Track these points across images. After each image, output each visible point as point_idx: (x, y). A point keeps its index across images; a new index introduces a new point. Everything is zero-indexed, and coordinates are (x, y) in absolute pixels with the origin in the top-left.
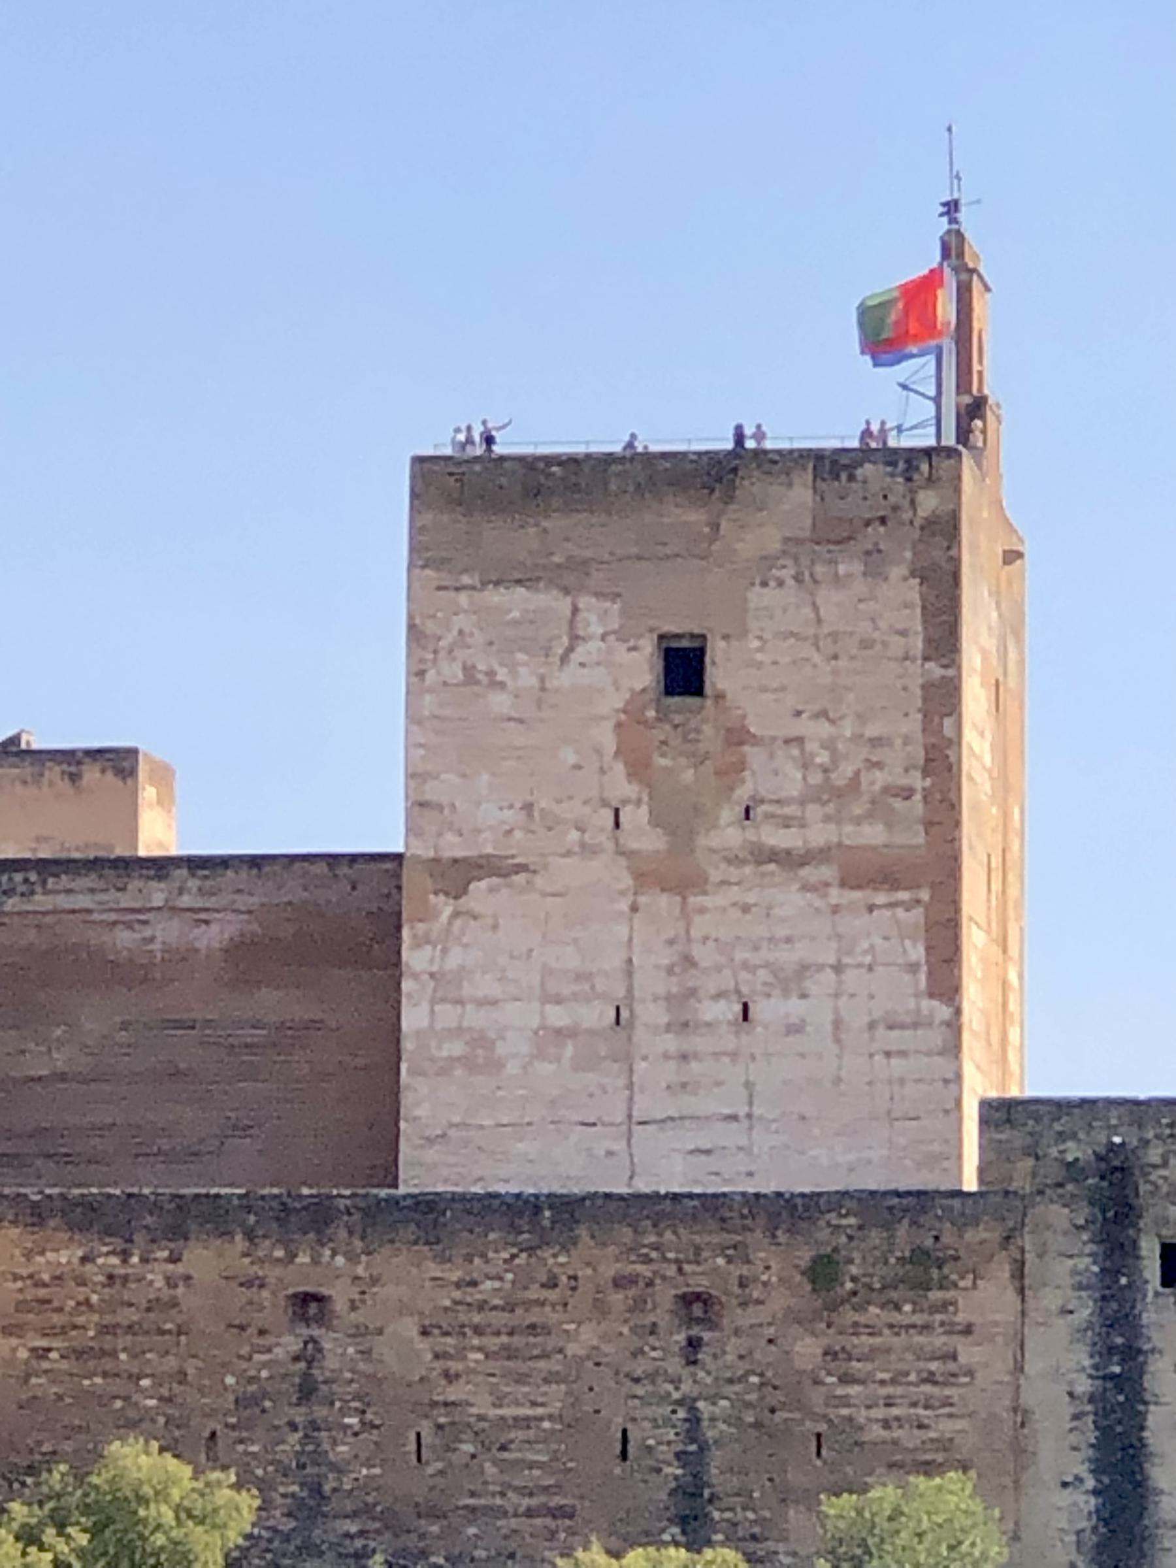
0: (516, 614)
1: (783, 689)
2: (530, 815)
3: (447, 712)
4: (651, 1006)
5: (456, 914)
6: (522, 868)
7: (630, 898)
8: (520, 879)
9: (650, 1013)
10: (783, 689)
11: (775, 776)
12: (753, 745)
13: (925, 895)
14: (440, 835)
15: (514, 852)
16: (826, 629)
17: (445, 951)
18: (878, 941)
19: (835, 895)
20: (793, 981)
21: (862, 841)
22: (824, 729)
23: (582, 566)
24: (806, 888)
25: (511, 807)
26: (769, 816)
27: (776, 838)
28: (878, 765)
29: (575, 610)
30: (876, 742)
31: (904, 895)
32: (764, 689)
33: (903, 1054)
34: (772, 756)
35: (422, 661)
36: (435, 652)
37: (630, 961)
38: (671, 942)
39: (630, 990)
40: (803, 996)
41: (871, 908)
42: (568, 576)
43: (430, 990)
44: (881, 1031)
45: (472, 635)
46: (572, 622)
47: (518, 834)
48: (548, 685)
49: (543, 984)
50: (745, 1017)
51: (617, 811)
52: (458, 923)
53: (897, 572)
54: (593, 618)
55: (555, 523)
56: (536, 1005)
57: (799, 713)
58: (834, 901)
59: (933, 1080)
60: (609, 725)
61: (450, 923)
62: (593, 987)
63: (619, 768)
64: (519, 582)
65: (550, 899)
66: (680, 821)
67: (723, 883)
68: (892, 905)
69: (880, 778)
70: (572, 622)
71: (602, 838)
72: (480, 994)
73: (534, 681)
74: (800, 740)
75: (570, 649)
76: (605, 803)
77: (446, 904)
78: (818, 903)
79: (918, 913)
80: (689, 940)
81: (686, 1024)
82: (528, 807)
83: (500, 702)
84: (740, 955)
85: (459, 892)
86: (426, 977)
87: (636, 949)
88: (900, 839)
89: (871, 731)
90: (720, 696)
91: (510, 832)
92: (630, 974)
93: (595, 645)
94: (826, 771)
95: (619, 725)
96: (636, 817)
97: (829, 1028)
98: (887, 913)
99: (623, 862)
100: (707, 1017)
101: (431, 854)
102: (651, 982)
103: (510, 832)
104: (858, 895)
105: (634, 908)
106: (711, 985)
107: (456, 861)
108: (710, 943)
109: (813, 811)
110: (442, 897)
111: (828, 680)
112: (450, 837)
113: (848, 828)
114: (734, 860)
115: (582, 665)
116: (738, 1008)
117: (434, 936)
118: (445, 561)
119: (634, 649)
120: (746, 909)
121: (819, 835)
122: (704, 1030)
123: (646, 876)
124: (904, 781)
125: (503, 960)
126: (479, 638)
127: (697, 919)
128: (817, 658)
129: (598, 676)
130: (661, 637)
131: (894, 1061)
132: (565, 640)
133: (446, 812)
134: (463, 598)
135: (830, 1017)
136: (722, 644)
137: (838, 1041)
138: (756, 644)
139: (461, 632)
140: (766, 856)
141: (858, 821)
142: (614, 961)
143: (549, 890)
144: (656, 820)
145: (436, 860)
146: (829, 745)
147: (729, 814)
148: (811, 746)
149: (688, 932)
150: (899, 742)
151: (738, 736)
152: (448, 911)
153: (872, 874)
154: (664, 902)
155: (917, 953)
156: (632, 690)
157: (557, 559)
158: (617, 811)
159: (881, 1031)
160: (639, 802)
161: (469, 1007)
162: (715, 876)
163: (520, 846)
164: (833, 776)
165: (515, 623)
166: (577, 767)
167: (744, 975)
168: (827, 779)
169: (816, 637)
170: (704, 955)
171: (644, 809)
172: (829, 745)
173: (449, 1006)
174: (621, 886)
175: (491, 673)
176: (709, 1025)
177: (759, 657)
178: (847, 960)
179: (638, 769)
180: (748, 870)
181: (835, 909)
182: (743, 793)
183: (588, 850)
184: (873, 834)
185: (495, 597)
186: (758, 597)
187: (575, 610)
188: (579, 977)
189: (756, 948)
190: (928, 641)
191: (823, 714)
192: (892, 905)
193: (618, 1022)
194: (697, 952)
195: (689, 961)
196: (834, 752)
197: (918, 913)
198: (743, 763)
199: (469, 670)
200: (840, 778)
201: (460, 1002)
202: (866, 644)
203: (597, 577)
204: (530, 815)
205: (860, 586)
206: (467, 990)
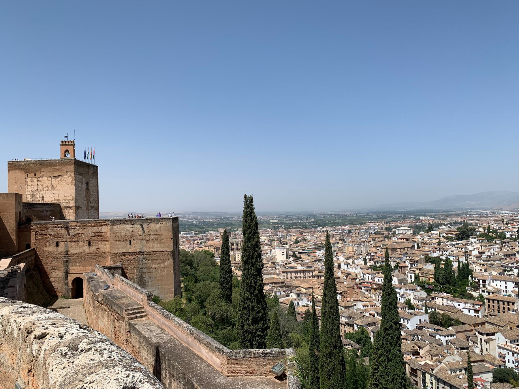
23: (82, 174)
140: (92, 207)
151: (90, 194)
186: (91, 179)
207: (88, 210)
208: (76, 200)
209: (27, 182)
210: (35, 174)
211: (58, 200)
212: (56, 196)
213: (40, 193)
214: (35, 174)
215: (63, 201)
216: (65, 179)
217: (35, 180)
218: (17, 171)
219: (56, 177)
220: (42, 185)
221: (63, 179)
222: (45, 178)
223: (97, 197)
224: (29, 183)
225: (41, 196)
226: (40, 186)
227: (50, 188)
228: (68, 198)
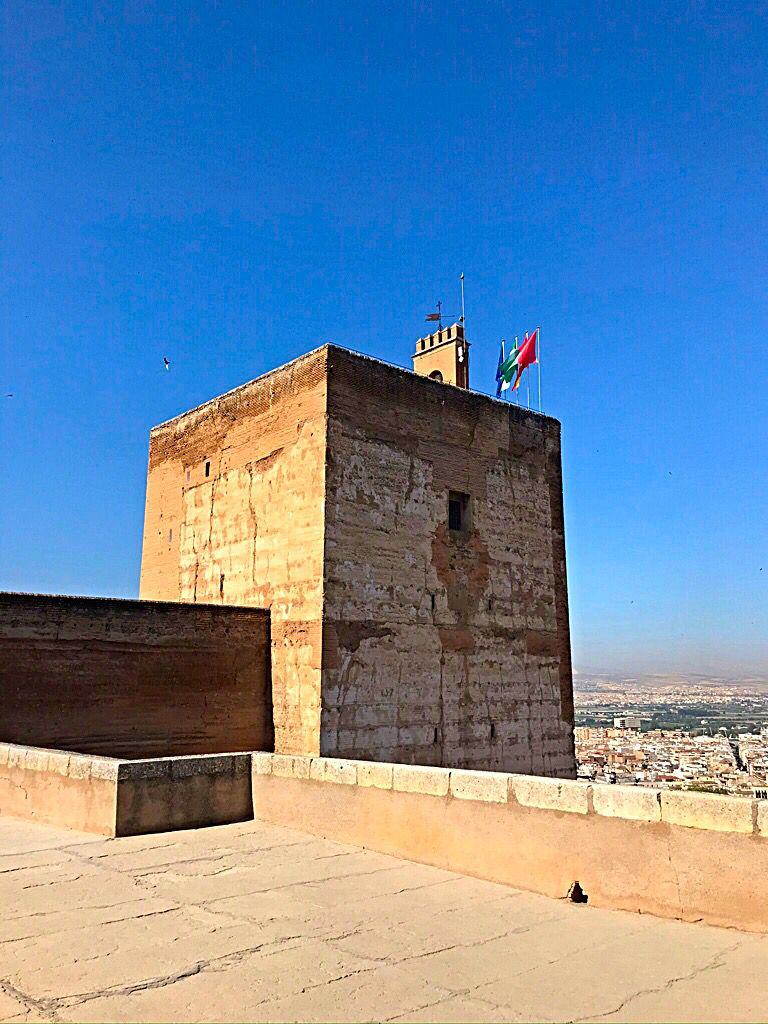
0: (383, 462)
1: (501, 534)
2: (391, 594)
3: (348, 518)
4: (451, 727)
5: (353, 663)
6: (388, 631)
7: (440, 656)
8: (386, 638)
9: (452, 733)
10: (501, 534)
11: (500, 585)
12: (491, 564)
13: (559, 661)
14: (343, 603)
15: (384, 619)
16: (517, 503)
17: (347, 689)
18: (543, 686)
19: (528, 659)
20: (511, 710)
21: (535, 627)
22: (516, 559)
24: (513, 654)
25: (382, 589)
26: (499, 607)
27: (504, 622)
28: (538, 584)
29: (412, 467)
30: (538, 570)
31: (551, 660)
32: (494, 533)
33: (555, 754)
34: (498, 572)
35: (335, 481)
36: (342, 476)
37: (441, 698)
38: (459, 685)
39: (441, 719)
40: (516, 720)
41: (540, 666)
42: (406, 443)
43: (336, 720)
44: (546, 742)
45: (361, 470)
46: (411, 473)
47: (385, 607)
48: (400, 511)
49: (398, 713)
50: (492, 736)
51: (433, 597)
52: (354, 669)
53: (541, 479)
54: (421, 474)
55: (402, 410)
56: (395, 729)
57: (508, 549)
58: (526, 661)
59: (566, 770)
60: (429, 541)
61: (349, 669)
62: (424, 716)
63: (434, 569)
64: (385, 442)
65: (402, 654)
66: (462, 609)
67: (481, 647)
68: (548, 665)
69: (539, 591)
70: (411, 473)
71: (427, 614)
72: (366, 724)
73: (393, 507)
74: (508, 565)
75: (410, 491)
76: (429, 593)
77: (347, 655)
78: (520, 662)
79: (555, 671)
80: (468, 684)
81: (467, 741)
82: (390, 589)
83: (374, 515)
84: (490, 694)
85: (353, 647)
86: (335, 710)
87: (445, 689)
88: (549, 627)
89: (536, 563)
90: (477, 533)
91: (381, 605)
92: (441, 707)
93: (421, 490)
94: (520, 584)
95: (433, 543)
96: (442, 602)
97: (527, 740)
98: (545, 669)
99: (436, 630)
100: (477, 735)
101: (339, 619)
102: (453, 714)
103: (381, 605)
104: (534, 658)
105: (442, 662)
106: (478, 713)
107: (351, 623)
108: (477, 686)
109: (516, 607)
110: (344, 651)
111: (517, 531)
112: (350, 606)
113: (529, 619)
114: (486, 635)
115: (416, 501)
116: (489, 728)
117: (339, 680)
118: (348, 419)
119: (438, 496)
120: (491, 664)
121: (518, 622)
122: (476, 743)
123: (448, 644)
124: (548, 594)
125: (378, 697)
126: (364, 474)
127: (472, 670)
128: (514, 520)
129: (422, 510)
130: (452, 493)
131: (553, 759)
132: (408, 484)
133: (347, 587)
134: (356, 444)
135: (527, 734)
136: (476, 502)
137: (530, 747)
138: (490, 505)
139: (355, 467)
140: (499, 632)
141: (532, 615)
142: (432, 699)
143: (402, 647)
144: (451, 607)
145: (342, 622)
146: (520, 567)
147: (482, 605)
148: (514, 568)
149: (467, 679)
150: (545, 571)
151: (485, 560)
152: (349, 659)
153: (539, 649)
154: (456, 659)
155: (557, 694)
156: (438, 521)
157: (402, 432)
158: (433, 597)
159: (546, 742)
160: (443, 593)
161: (360, 732)
162: (478, 644)
163: (387, 616)
164: (523, 587)
165: (383, 468)
166: (414, 566)
167: (492, 707)
168: (520, 589)
169: (513, 506)
170: (474, 692)
171: (446, 595)
172: (520, 567)
173: (347, 733)
174: (436, 647)
175: (372, 498)
176: (479, 740)
177: (492, 513)
178: (533, 698)
179: (441, 572)
180: (491, 640)
181: (527, 666)
182: (488, 592)
183: (420, 621)
184: (538, 623)
185: (372, 448)
186: (492, 479)
187: (412, 467)
188: (418, 709)
189: (496, 691)
190: (553, 518)
191: (516, 551)
192: (548, 665)
193: (435, 740)
194: (472, 691)
195: (467, 696)
196: (522, 573)
197: (555, 671)
198: (488, 574)
199: (360, 492)
200: (525, 588)
201: (354, 729)
202: (532, 515)
203: (421, 449)
204: (391, 594)
205: (529, 484)
206: (358, 719)
207: (466, 648)
208: (330, 583)
209: (184, 508)
210: (208, 465)
211: (266, 589)
212: (261, 563)
213: (218, 554)
214: (208, 465)
215: (281, 594)
216: (294, 469)
217: (206, 492)
218: (167, 464)
219: (265, 462)
220: (222, 516)
221: (284, 472)
222: (233, 475)
223: (548, 578)
224: (193, 513)
225: (217, 571)
226: (216, 522)
227: (244, 527)
228: (298, 574)
